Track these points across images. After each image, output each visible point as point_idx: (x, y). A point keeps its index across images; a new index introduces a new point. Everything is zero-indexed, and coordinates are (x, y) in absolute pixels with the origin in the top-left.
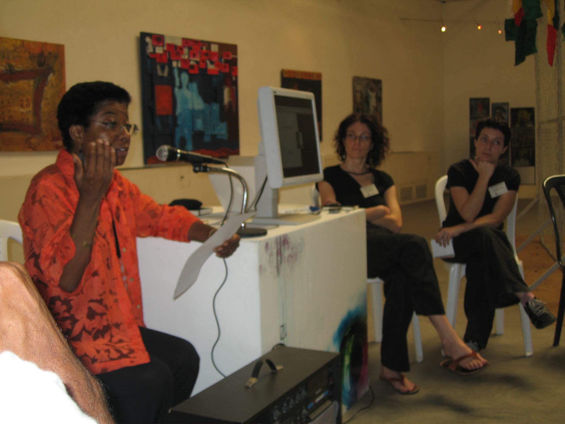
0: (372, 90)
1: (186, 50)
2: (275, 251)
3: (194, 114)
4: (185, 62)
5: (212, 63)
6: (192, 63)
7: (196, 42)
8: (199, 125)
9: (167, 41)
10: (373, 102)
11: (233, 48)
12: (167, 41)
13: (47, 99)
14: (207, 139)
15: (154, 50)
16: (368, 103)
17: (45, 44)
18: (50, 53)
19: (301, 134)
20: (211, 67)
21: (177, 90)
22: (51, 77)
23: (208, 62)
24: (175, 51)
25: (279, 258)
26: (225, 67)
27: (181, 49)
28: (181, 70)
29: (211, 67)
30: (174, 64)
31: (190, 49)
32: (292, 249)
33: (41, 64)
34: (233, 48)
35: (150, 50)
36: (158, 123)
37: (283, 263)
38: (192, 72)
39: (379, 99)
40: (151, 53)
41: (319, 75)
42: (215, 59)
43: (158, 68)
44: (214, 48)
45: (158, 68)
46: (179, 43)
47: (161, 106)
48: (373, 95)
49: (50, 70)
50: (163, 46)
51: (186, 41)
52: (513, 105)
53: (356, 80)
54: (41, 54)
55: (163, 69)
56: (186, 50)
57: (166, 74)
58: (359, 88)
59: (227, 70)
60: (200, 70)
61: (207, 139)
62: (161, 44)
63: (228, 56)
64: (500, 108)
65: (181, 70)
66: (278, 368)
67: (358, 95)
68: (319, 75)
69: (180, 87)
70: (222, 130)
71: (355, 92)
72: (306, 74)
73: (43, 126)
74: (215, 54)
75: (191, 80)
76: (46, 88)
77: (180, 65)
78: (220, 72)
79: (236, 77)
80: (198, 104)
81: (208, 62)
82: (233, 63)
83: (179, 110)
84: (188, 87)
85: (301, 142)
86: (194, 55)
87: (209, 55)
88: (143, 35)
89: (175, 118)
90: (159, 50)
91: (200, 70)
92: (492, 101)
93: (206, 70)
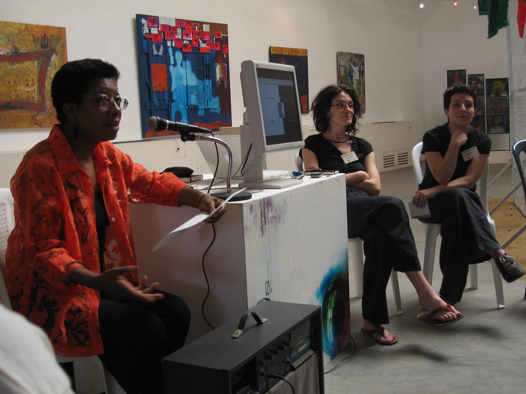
0: (355, 65)
2: (259, 213)
4: (177, 40)
5: (204, 42)
6: (185, 42)
8: (193, 100)
10: (356, 76)
13: (50, 78)
14: (201, 113)
16: (351, 77)
18: (52, 36)
19: (282, 104)
20: (203, 45)
21: (171, 67)
22: (54, 58)
26: (216, 45)
28: (175, 49)
29: (203, 45)
30: (169, 44)
32: (275, 211)
33: (44, 46)
36: (155, 98)
37: (267, 224)
38: (185, 50)
39: (362, 73)
40: (146, 33)
41: (306, 50)
43: (154, 47)
45: (154, 47)
48: (356, 69)
49: (52, 51)
52: (487, 77)
53: (340, 55)
54: (44, 37)
57: (161, 53)
58: (342, 63)
59: (218, 49)
60: (193, 48)
61: (201, 113)
63: (219, 35)
64: (476, 78)
65: (175, 49)
66: (264, 320)
67: (342, 69)
68: (306, 50)
69: (175, 65)
70: (215, 104)
71: (338, 66)
72: (292, 50)
74: (206, 33)
75: (184, 59)
76: (49, 68)
77: (174, 45)
78: (211, 50)
79: (227, 55)
80: (192, 80)
82: (224, 42)
83: (173, 88)
84: (182, 65)
85: (283, 112)
86: (187, 36)
87: (201, 34)
89: (171, 94)
91: (193, 48)
92: (468, 73)
93: (199, 48)
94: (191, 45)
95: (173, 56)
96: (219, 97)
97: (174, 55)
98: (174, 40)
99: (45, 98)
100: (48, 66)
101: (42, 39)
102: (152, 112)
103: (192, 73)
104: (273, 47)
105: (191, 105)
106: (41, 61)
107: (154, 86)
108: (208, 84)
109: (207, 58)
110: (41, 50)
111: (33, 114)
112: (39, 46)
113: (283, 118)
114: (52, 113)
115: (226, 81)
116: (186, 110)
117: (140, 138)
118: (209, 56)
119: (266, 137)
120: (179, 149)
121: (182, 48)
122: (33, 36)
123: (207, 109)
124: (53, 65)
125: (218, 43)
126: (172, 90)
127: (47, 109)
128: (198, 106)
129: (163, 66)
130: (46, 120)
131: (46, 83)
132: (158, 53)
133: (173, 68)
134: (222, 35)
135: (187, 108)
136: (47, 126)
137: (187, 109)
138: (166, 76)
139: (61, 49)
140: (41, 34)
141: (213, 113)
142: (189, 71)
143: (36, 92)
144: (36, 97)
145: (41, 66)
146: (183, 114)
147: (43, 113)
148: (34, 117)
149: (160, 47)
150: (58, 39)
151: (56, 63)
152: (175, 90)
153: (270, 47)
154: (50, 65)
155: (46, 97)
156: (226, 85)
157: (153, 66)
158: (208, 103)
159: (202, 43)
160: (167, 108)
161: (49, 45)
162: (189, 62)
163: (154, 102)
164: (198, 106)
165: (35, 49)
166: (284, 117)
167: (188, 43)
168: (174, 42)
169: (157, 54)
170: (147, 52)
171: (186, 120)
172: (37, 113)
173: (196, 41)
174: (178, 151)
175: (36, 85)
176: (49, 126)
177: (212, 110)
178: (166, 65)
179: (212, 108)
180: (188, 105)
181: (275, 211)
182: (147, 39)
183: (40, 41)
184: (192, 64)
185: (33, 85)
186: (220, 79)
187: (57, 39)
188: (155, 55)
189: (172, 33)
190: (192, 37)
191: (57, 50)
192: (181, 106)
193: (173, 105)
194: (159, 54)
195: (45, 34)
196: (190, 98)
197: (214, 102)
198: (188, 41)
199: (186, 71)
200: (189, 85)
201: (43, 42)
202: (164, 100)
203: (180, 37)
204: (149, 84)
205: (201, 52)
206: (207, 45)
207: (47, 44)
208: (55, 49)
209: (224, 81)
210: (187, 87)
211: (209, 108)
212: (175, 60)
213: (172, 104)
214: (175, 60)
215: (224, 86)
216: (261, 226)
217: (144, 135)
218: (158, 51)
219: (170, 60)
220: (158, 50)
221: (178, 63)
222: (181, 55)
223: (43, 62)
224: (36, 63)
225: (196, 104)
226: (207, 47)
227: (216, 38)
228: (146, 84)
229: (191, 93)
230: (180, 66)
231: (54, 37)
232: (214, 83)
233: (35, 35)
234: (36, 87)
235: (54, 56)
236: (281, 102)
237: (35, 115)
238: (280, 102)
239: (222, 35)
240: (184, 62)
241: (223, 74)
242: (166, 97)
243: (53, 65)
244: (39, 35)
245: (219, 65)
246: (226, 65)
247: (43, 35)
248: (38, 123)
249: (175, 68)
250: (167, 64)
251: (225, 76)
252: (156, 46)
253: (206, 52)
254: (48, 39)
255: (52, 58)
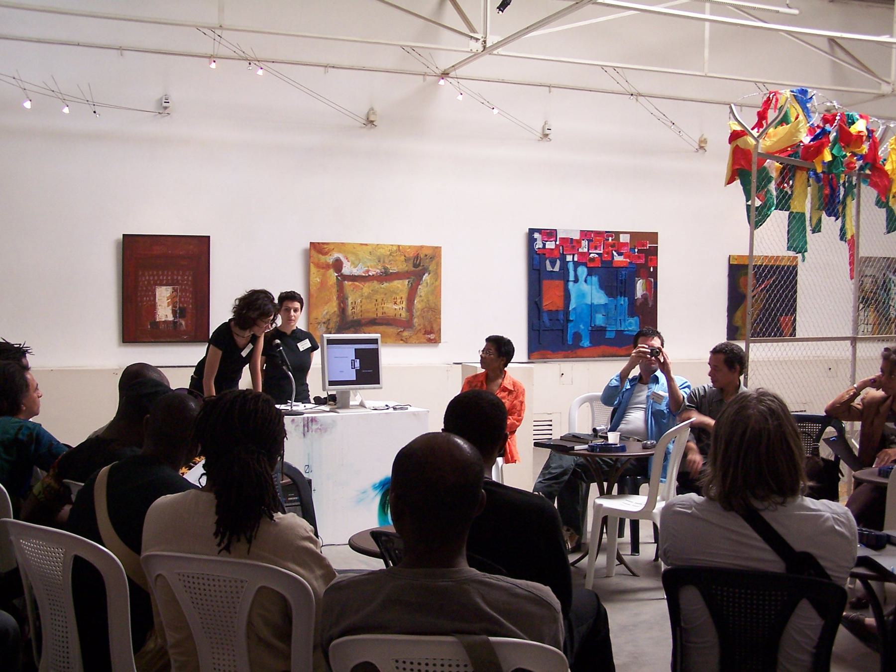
1: (585, 243)
2: (302, 424)
3: (593, 309)
4: (583, 254)
5: (620, 254)
6: (591, 256)
7: (598, 233)
8: (600, 320)
9: (560, 235)
11: (653, 237)
12: (560, 235)
13: (421, 296)
15: (544, 245)
17: (422, 247)
18: (426, 256)
19: (358, 360)
20: (618, 258)
21: (571, 284)
22: (426, 277)
23: (615, 253)
24: (570, 244)
25: (306, 429)
26: (639, 257)
27: (579, 242)
28: (576, 265)
29: (618, 258)
30: (569, 258)
31: (589, 241)
33: (415, 266)
34: (653, 237)
35: (539, 245)
36: (545, 318)
37: (310, 432)
40: (539, 248)
42: (624, 250)
43: (548, 262)
44: (625, 239)
45: (548, 262)
46: (577, 236)
47: (551, 300)
49: (425, 270)
50: (556, 241)
51: (585, 234)
55: (553, 264)
56: (585, 243)
57: (557, 269)
59: (642, 261)
60: (603, 262)
61: (610, 335)
62: (552, 240)
65: (576, 265)
69: (576, 281)
73: (416, 320)
74: (625, 244)
75: (590, 274)
76: (420, 287)
77: (576, 259)
79: (656, 269)
80: (600, 298)
81: (615, 253)
82: (654, 251)
84: (586, 281)
86: (596, 249)
87: (618, 247)
88: (532, 231)
89: (566, 312)
90: (550, 245)
91: (603, 262)
94: (600, 258)
95: (573, 272)
96: (639, 317)
97: (575, 271)
98: (558, 258)
99: (413, 315)
100: (419, 285)
101: (414, 259)
102: (541, 331)
103: (600, 290)
104: (733, 256)
105: (595, 325)
106: (411, 280)
107: (544, 304)
108: (622, 302)
109: (624, 273)
110: (414, 269)
111: (399, 331)
112: (411, 265)
113: (356, 370)
114: (420, 329)
115: (652, 299)
116: (589, 332)
117: (526, 360)
118: (626, 271)
119: (329, 381)
120: (563, 374)
121: (586, 263)
122: (405, 257)
123: (619, 330)
124: (424, 284)
125: (640, 255)
126: (570, 309)
127: (415, 326)
128: (606, 327)
129: (560, 283)
130: (413, 337)
131: (416, 301)
132: (553, 268)
133: (574, 285)
134: (648, 245)
135: (590, 328)
136: (414, 342)
137: (591, 330)
138: (562, 294)
139: (435, 268)
140: (414, 254)
141: (627, 335)
142: (596, 288)
143: (404, 309)
144: (404, 314)
145: (412, 284)
146: (583, 336)
147: (410, 329)
148: (401, 333)
149: (556, 261)
150: (432, 258)
151: (428, 281)
152: (574, 309)
153: (730, 256)
154: (422, 284)
155: (414, 314)
156: (650, 304)
157: (546, 283)
158: (621, 324)
159: (617, 255)
160: (561, 328)
161: (421, 265)
162: (595, 277)
163: (543, 321)
164: (606, 327)
165: (406, 269)
166: (358, 368)
167: (597, 256)
168: (576, 256)
169: (552, 270)
170: (538, 268)
171: (588, 342)
172: (404, 330)
173: (607, 253)
174: (562, 376)
175: (404, 303)
176: (415, 343)
177: (625, 333)
178: (562, 282)
179: (626, 329)
180: (591, 326)
181: (321, 425)
182: (539, 254)
183: (412, 261)
184: (600, 281)
185: (401, 303)
186: (642, 296)
187: (431, 258)
188: (548, 271)
189: (573, 246)
190: (603, 249)
191: (430, 268)
192: (582, 326)
193: (570, 325)
194: (554, 270)
195: (418, 254)
196: (595, 317)
197: (630, 323)
198: (597, 254)
199: (592, 287)
200: (594, 304)
201: (415, 262)
202: (559, 320)
203: (586, 250)
204: (538, 303)
205: (614, 266)
206: (625, 258)
207: (420, 263)
208: (428, 268)
209: (649, 299)
210: (592, 305)
211: (623, 329)
212: (576, 276)
213: (569, 324)
214: (576, 276)
215: (648, 304)
216: (303, 432)
217: (529, 358)
218: (553, 265)
219: (569, 276)
220: (553, 265)
221: (580, 279)
222: (585, 270)
223: (413, 281)
224: (406, 282)
225: (603, 325)
226: (624, 260)
227: (638, 250)
228: (536, 303)
229: (596, 312)
230: (584, 283)
231: (427, 257)
232: (632, 300)
233: (407, 256)
234: (404, 305)
235: (426, 275)
236: (356, 358)
237: (401, 331)
238: (354, 359)
239: (648, 245)
240: (589, 278)
241: (646, 290)
242: (561, 317)
243: (424, 284)
244: (411, 255)
245: (641, 280)
246: (652, 280)
247: (415, 255)
248: (405, 339)
249: (576, 285)
250: (564, 280)
251: (650, 292)
252: (550, 262)
253: (622, 266)
254: (420, 260)
255: (424, 277)
